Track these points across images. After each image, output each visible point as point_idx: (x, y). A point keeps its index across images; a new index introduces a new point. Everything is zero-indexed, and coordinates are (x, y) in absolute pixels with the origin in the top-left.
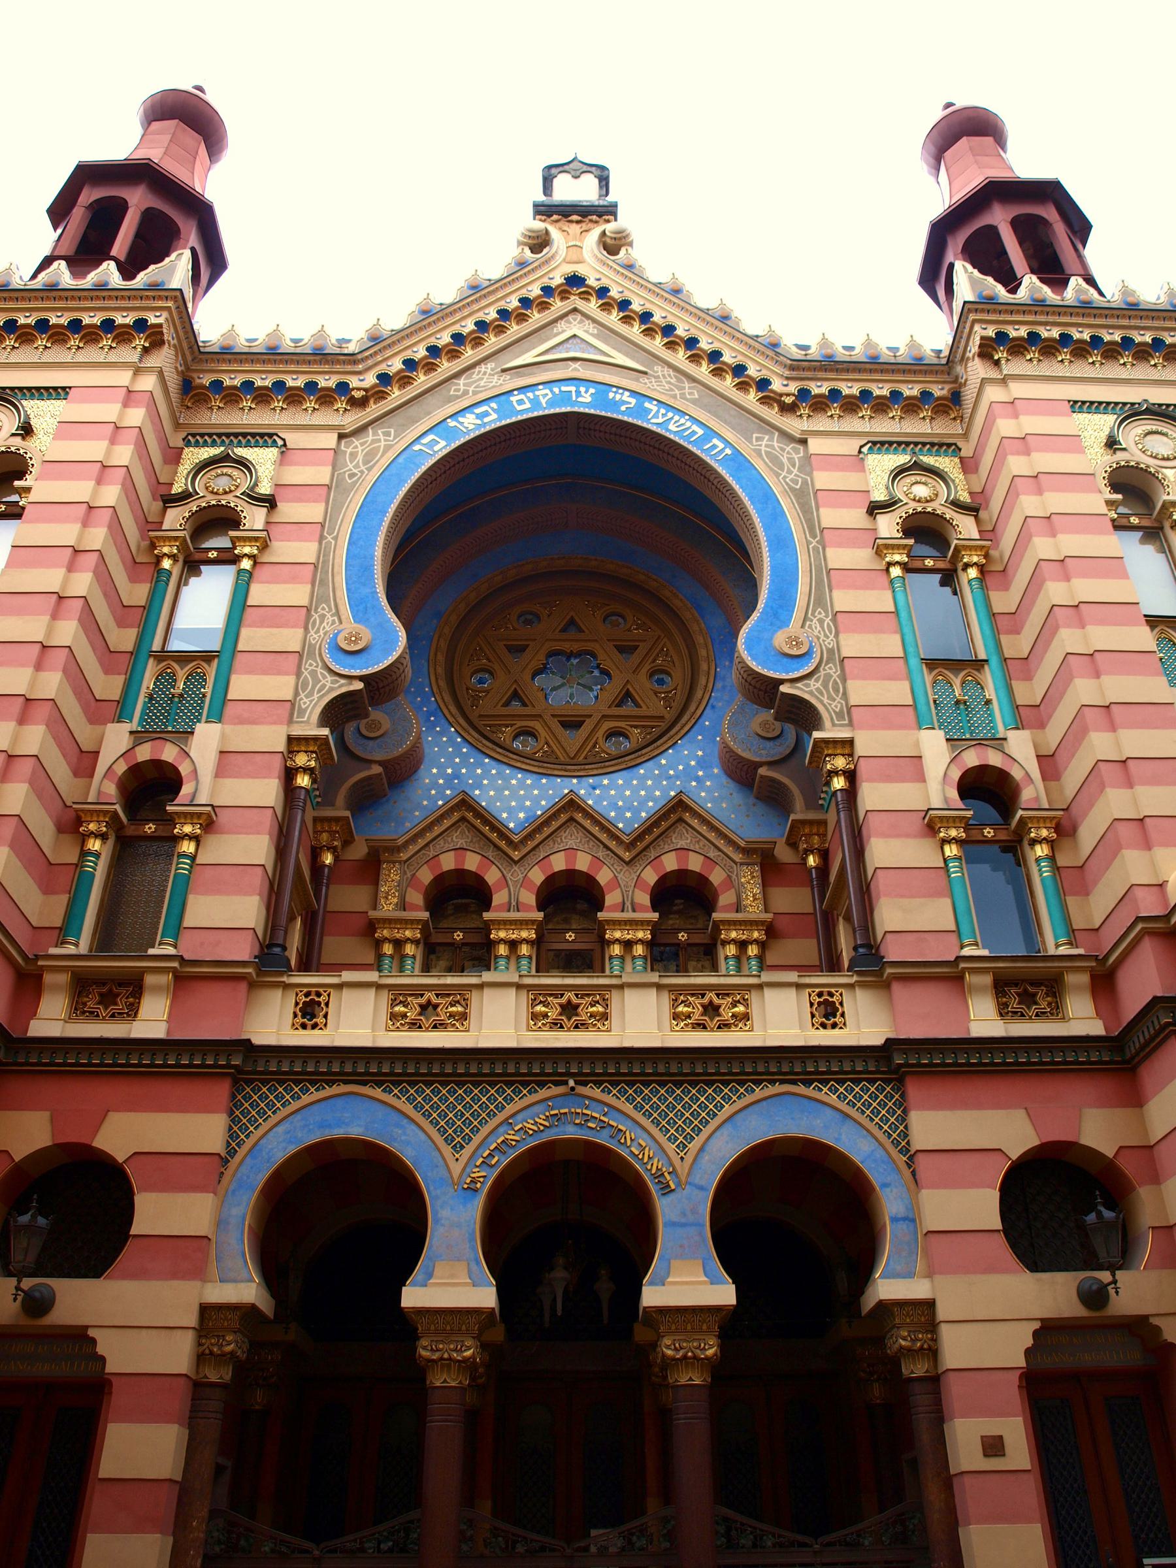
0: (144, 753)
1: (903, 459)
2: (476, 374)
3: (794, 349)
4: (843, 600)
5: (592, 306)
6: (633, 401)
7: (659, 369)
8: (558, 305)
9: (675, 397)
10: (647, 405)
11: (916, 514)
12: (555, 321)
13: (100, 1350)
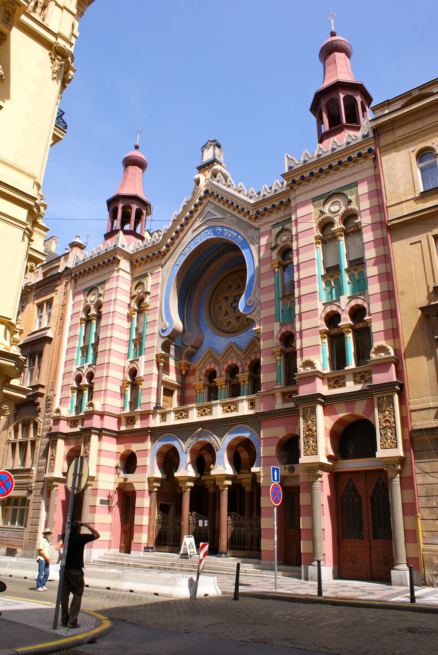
0: (131, 367)
1: (279, 229)
2: (188, 235)
3: (257, 196)
4: (263, 284)
5: (211, 199)
6: (221, 229)
7: (227, 215)
8: (205, 201)
9: (230, 224)
10: (224, 230)
11: (283, 247)
12: (204, 207)
13: (134, 486)
